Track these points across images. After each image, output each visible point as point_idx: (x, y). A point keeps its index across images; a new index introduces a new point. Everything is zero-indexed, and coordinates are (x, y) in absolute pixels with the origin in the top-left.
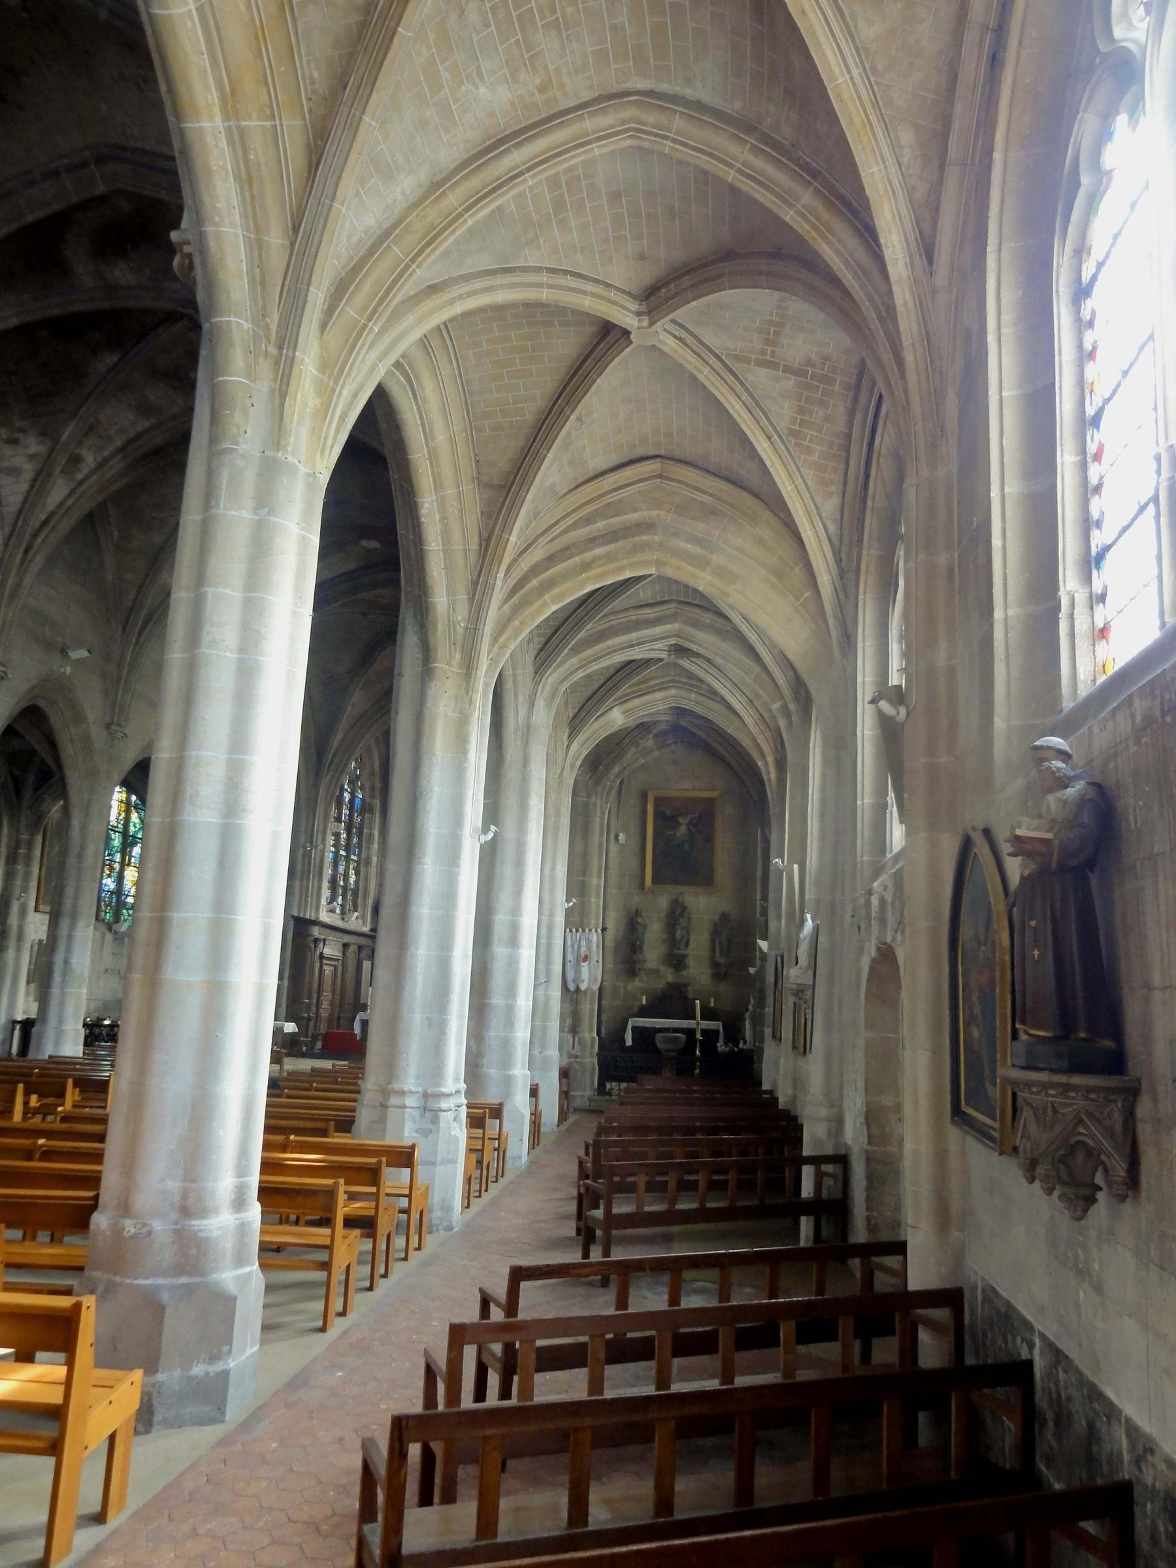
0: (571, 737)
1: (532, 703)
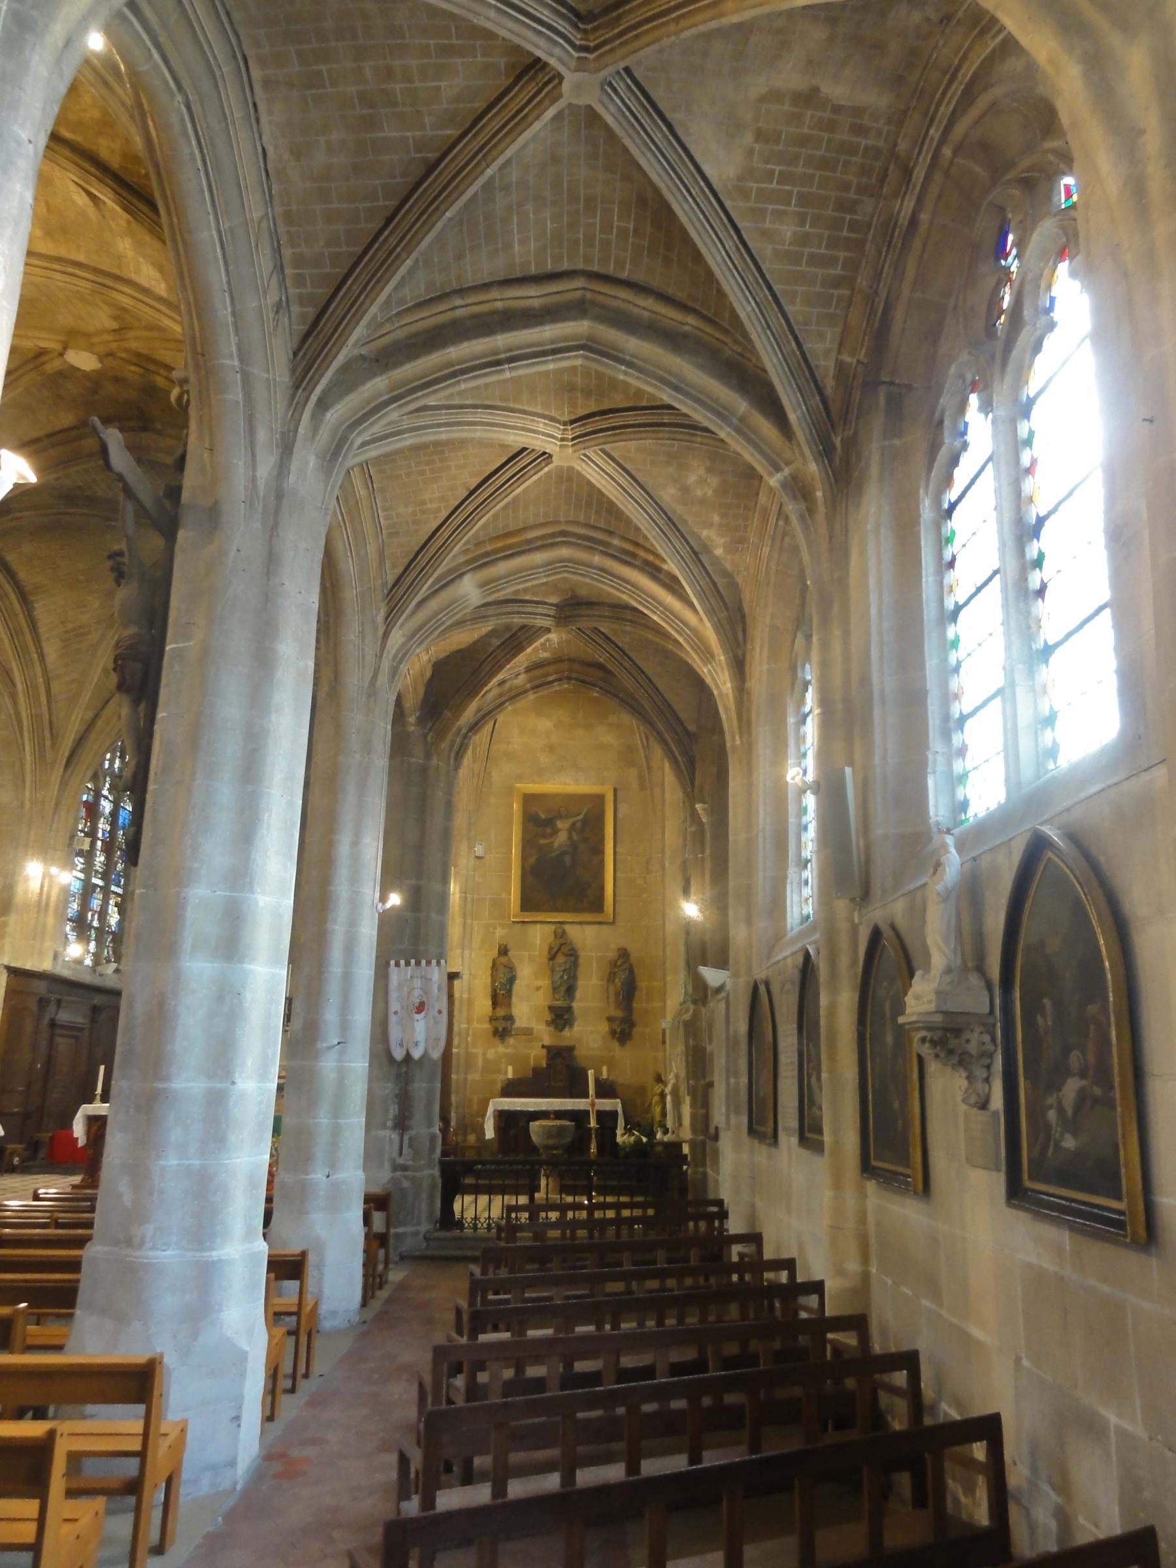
0: (390, 619)
1: (287, 448)
